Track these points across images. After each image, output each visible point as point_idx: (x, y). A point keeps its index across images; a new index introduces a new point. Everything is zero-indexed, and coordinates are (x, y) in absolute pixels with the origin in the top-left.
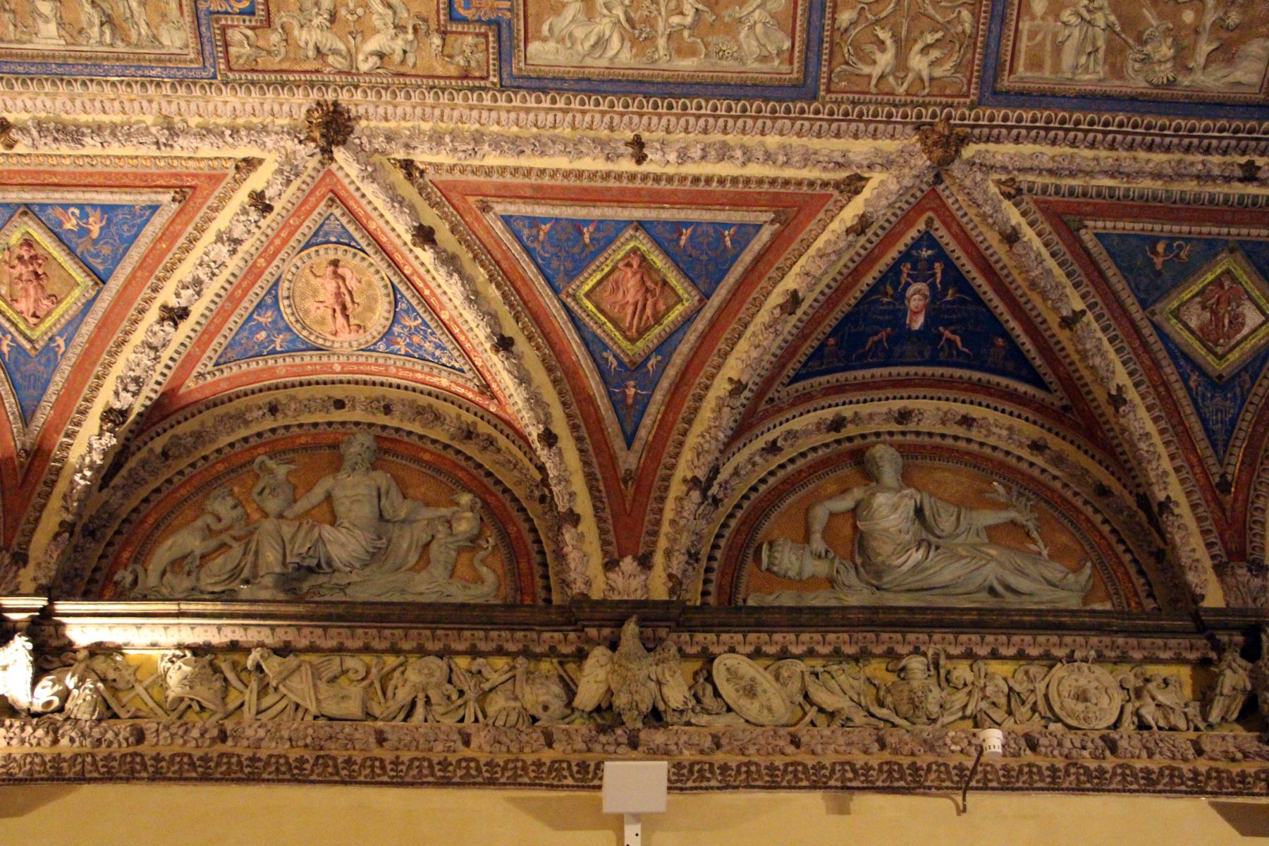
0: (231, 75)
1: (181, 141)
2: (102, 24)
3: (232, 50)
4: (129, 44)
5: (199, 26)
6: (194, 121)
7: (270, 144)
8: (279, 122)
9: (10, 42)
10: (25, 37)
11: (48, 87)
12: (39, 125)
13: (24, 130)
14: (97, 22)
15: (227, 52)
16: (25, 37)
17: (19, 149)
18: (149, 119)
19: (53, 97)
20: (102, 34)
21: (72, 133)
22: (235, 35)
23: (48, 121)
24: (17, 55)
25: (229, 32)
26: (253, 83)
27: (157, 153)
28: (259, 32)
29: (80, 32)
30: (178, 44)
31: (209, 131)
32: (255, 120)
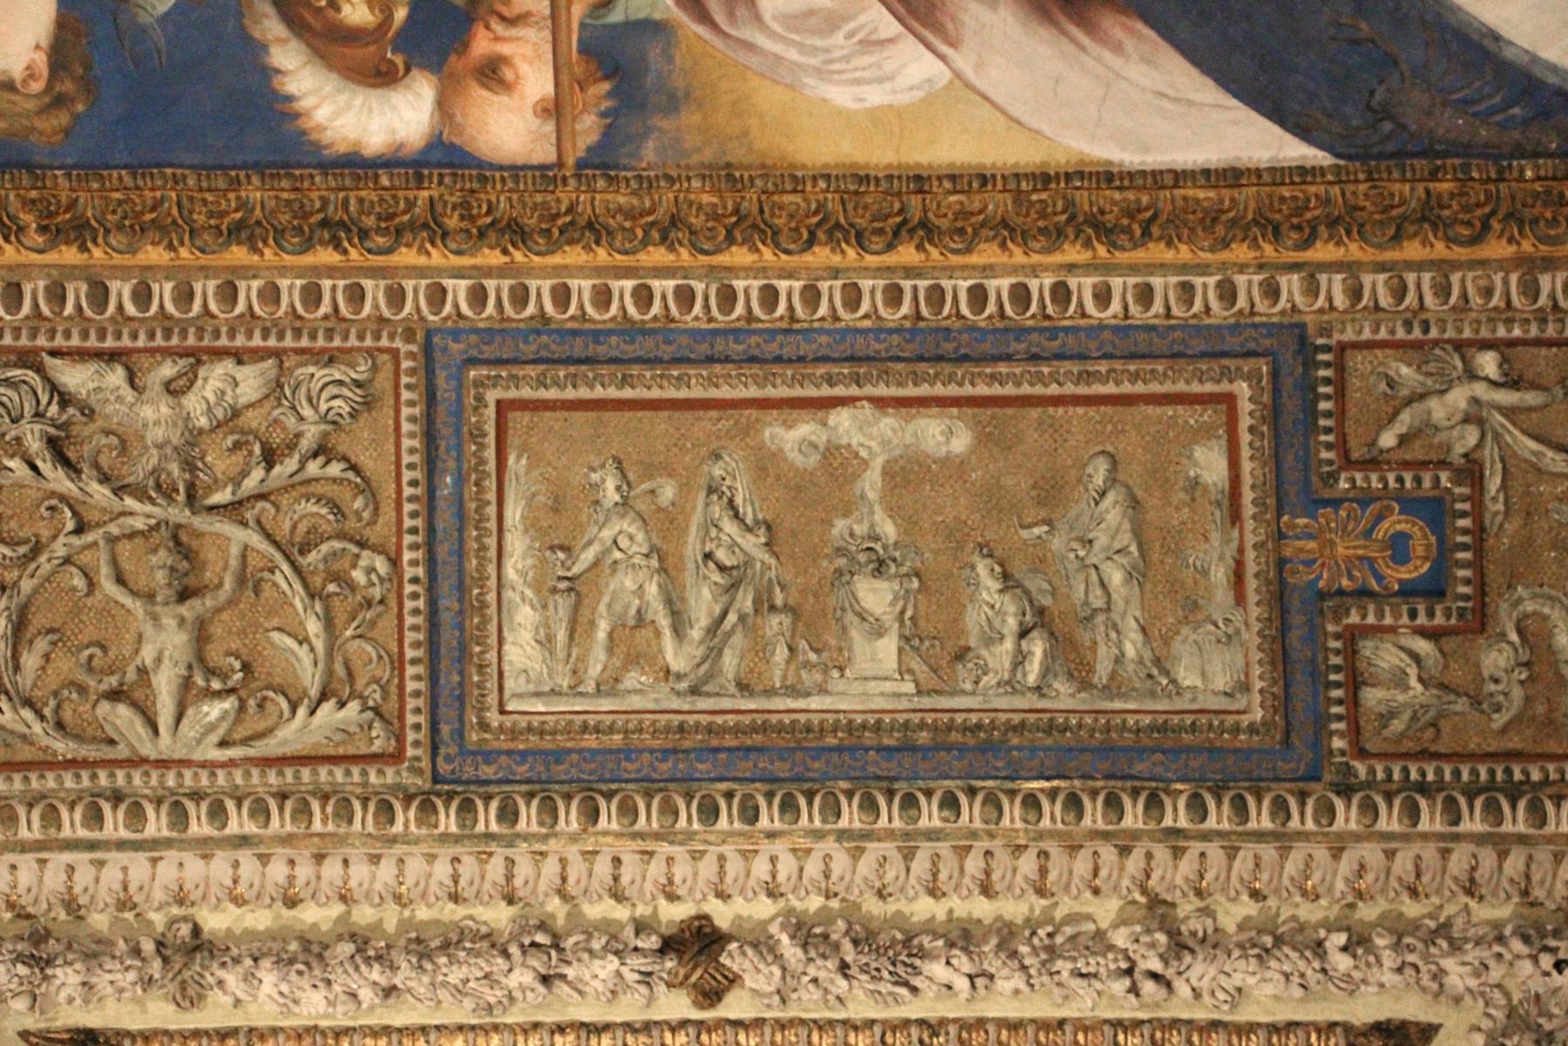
0: (1361, 768)
1: (1200, 971)
2: (1024, 633)
3: (1372, 697)
4: (1085, 685)
5: (1284, 629)
6: (1234, 913)
7: (1457, 975)
8: (1484, 912)
9: (769, 692)
10: (809, 678)
11: (851, 817)
12: (806, 932)
13: (762, 944)
14: (1012, 623)
15: (1354, 701)
16: (809, 678)
17: (735, 1006)
18: (1105, 911)
19: (856, 841)
20: (1020, 658)
21: (895, 951)
22: (1384, 656)
23: (825, 916)
24: (780, 728)
25: (1367, 647)
26: (1422, 788)
27: (1129, 1010)
28: (1450, 643)
29: (961, 655)
30: (1221, 682)
31: (1279, 941)
32: (1411, 909)
